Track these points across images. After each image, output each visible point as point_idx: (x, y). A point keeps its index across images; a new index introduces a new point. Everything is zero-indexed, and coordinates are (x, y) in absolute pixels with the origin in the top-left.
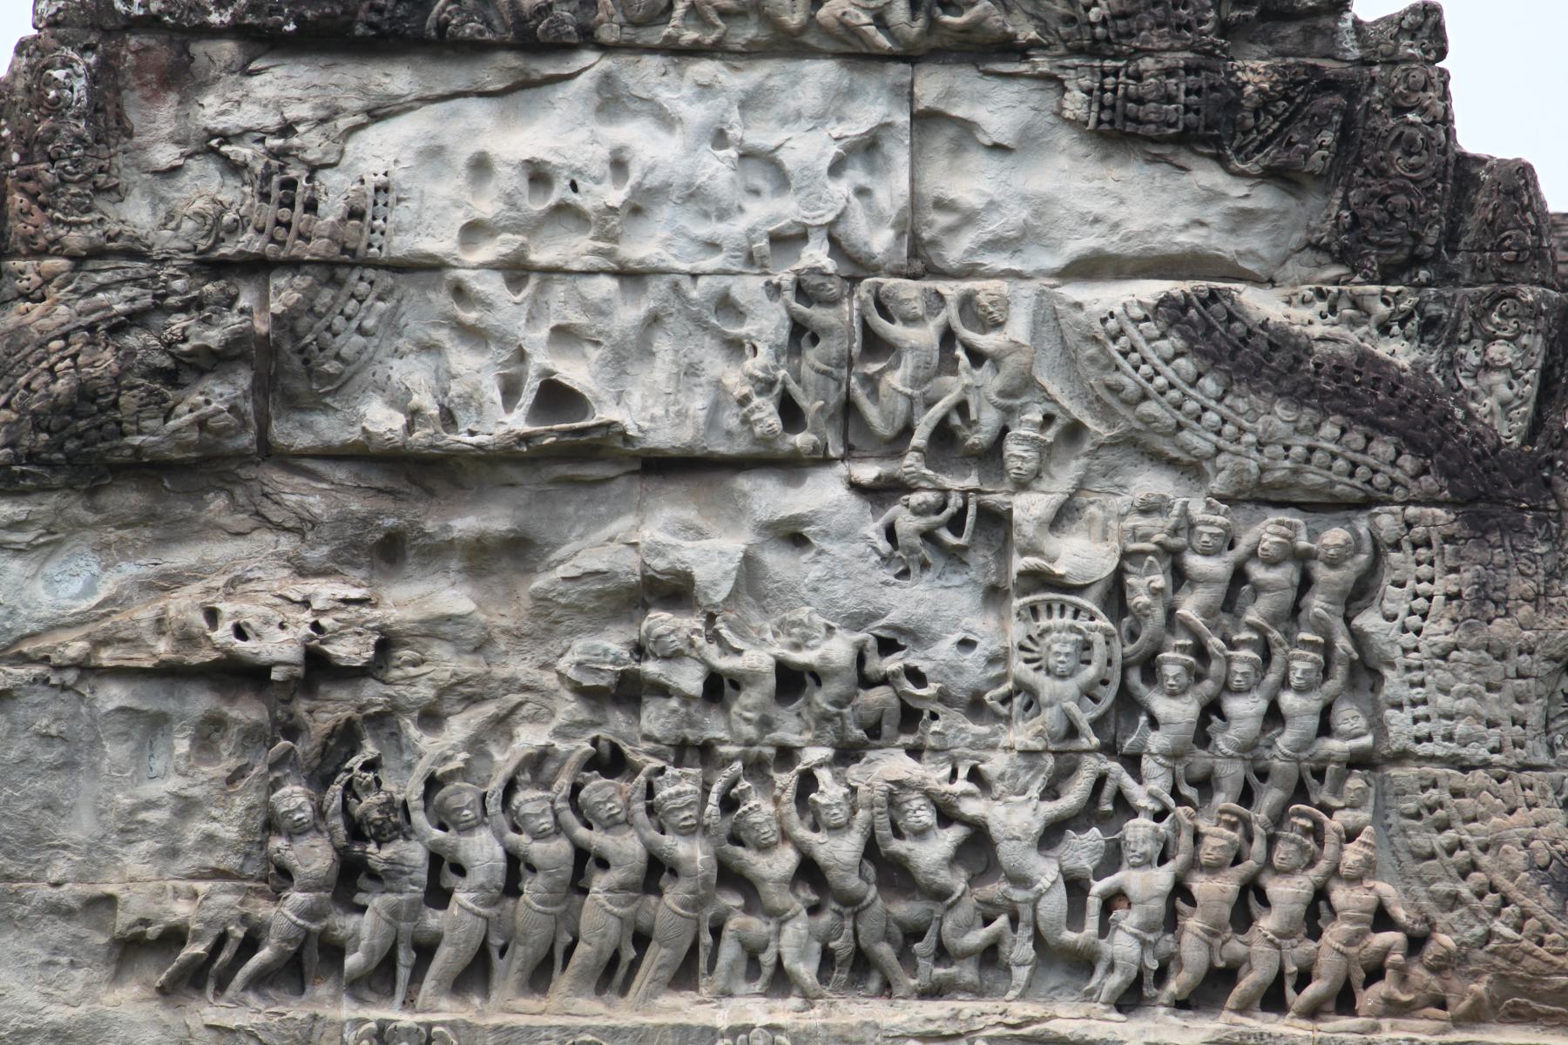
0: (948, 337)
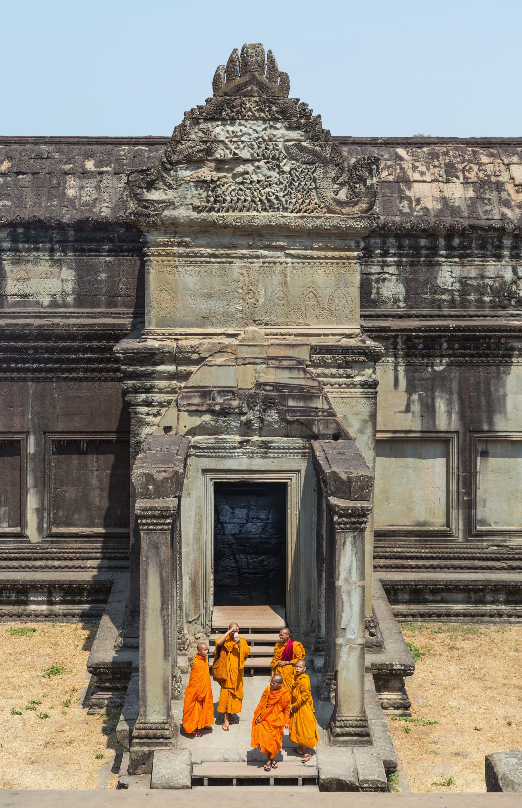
0: (273, 147)
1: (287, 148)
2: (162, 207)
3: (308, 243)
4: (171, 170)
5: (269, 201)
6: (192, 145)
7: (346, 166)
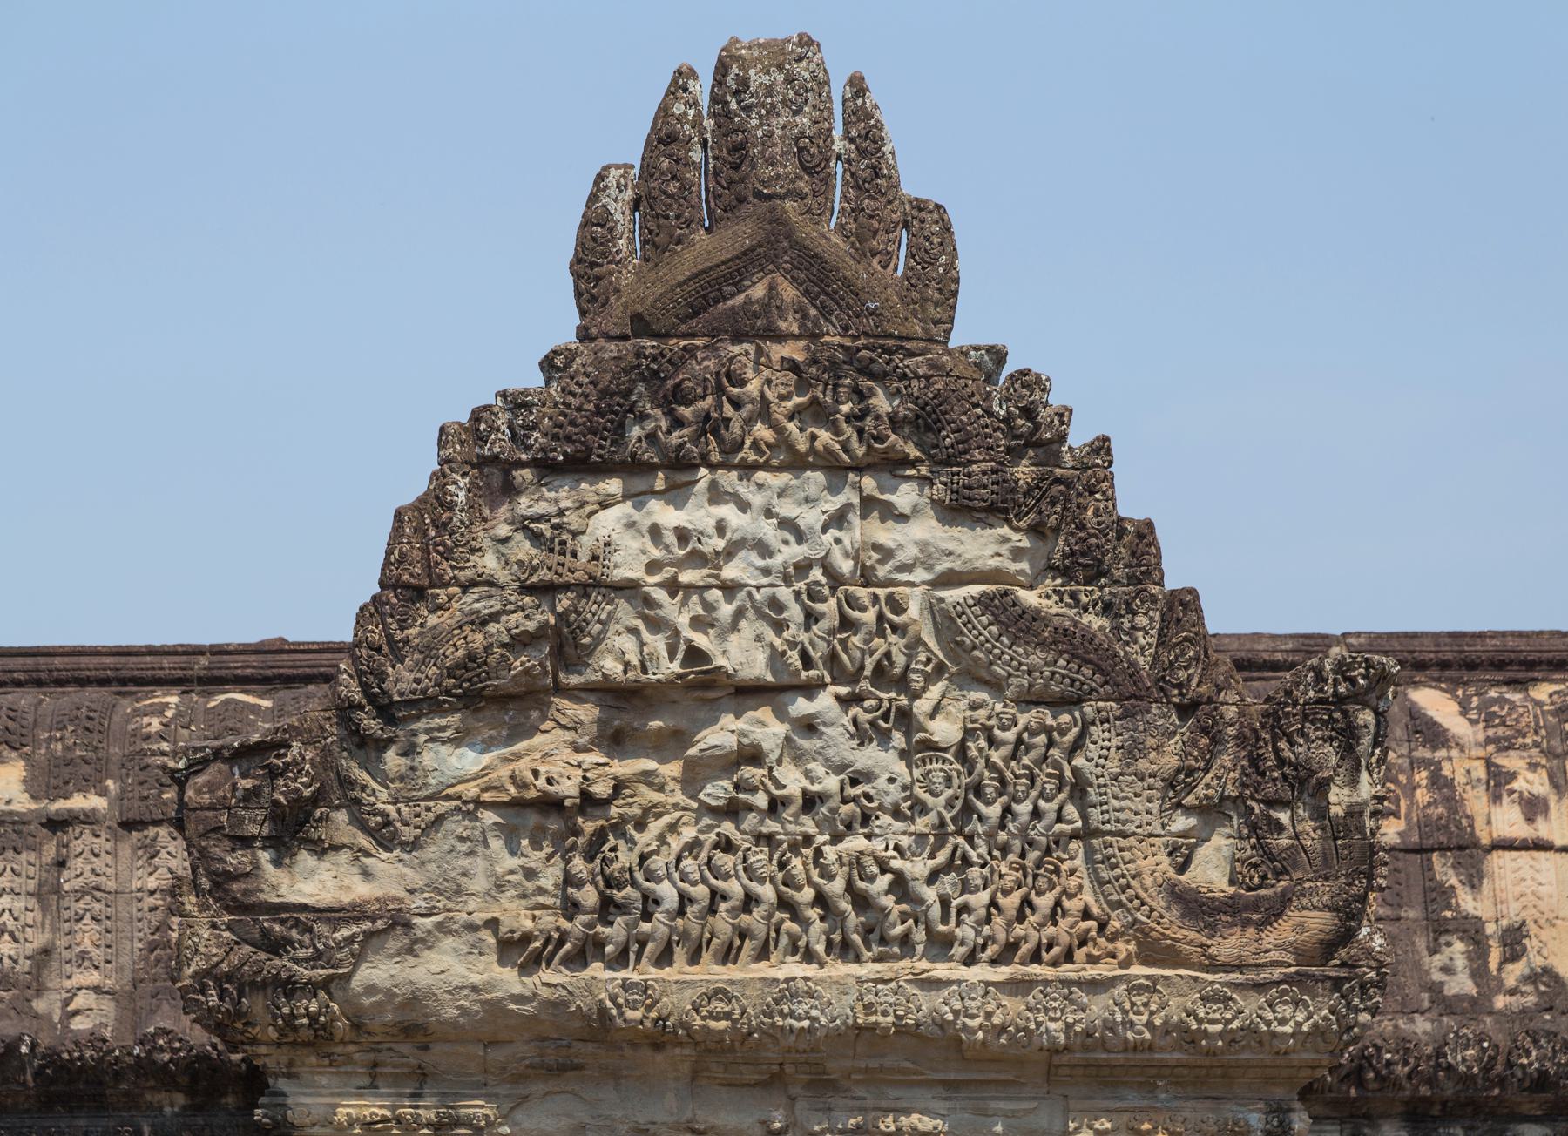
0: (881, 617)
1: (945, 621)
4: (383, 745)
5: (862, 902)
7: (1231, 712)
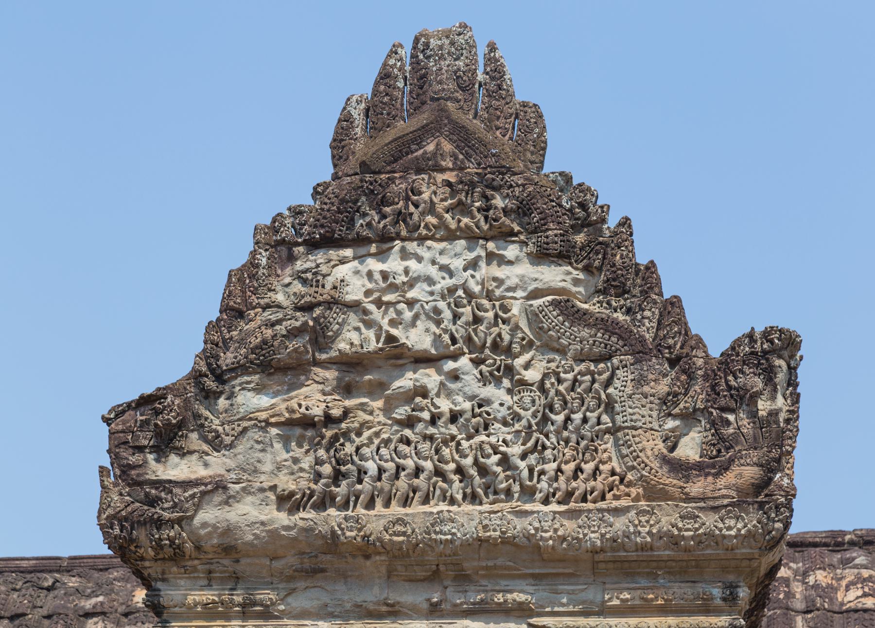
0: (496, 316)
1: (534, 317)
2: (193, 496)
3: (592, 594)
4: (218, 395)
5: (483, 471)
6: (273, 318)
7: (700, 362)
